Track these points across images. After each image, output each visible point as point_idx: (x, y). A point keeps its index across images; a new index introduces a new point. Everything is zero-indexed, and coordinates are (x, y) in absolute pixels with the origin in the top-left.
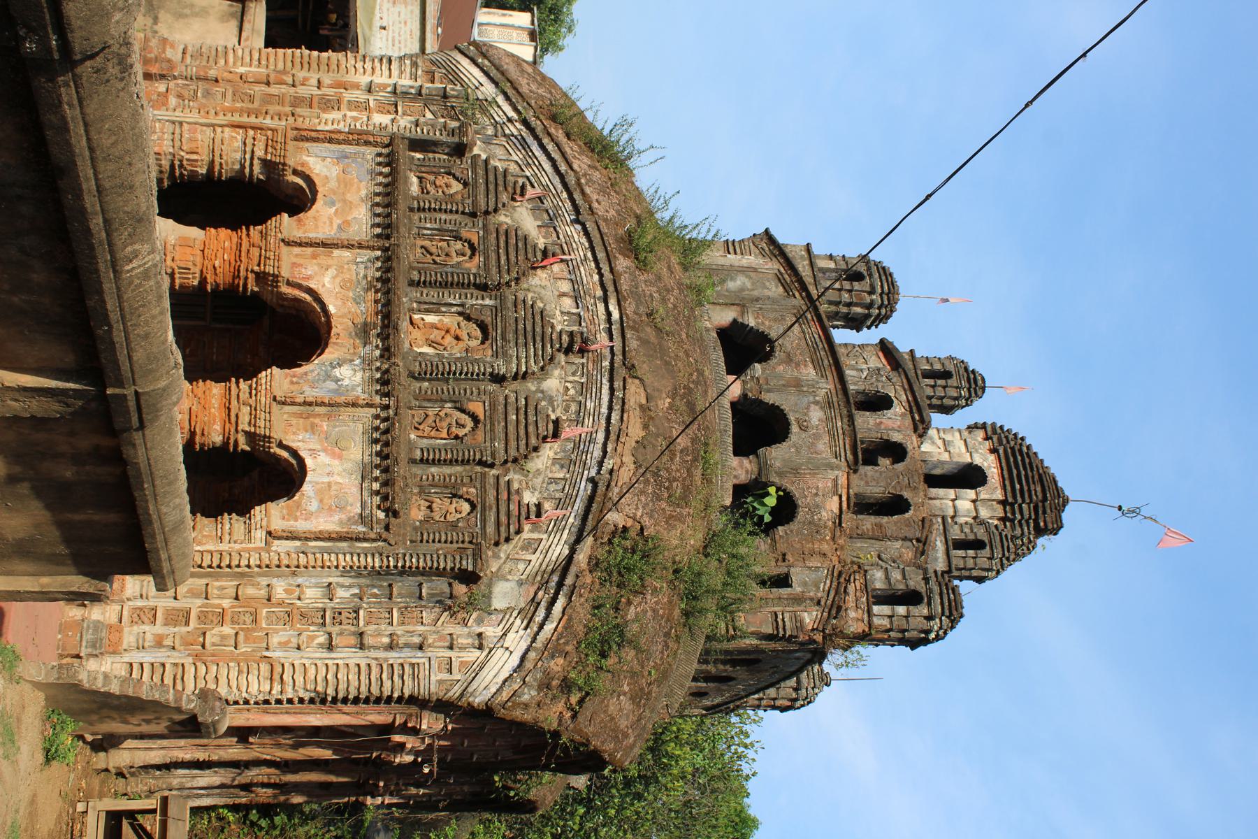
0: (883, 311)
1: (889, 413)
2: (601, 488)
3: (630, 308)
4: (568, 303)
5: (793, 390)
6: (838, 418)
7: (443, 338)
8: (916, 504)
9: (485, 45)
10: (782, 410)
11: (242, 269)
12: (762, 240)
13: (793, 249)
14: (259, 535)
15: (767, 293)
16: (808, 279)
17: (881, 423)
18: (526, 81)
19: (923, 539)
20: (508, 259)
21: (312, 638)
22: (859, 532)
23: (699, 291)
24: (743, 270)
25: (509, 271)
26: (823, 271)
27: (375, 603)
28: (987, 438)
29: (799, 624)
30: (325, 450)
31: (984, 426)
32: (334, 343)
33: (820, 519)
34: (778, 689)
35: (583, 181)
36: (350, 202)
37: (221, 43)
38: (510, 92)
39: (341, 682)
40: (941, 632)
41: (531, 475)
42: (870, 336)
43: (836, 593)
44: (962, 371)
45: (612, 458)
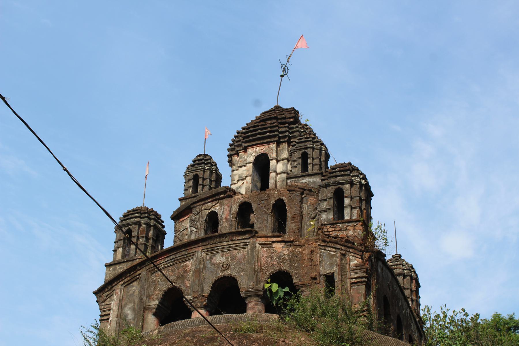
0: (152, 217)
1: (220, 213)
5: (202, 275)
6: (221, 244)
8: (279, 195)
10: (216, 281)
12: (101, 296)
13: (108, 275)
15: (136, 293)
16: (129, 265)
17: (226, 218)
19: (301, 190)
22: (297, 231)
23: (133, 338)
26: (124, 255)
28: (237, 154)
29: (359, 268)
31: (230, 156)
33: (288, 255)
34: (404, 288)
40: (361, 176)
42: (169, 226)
43: (337, 243)
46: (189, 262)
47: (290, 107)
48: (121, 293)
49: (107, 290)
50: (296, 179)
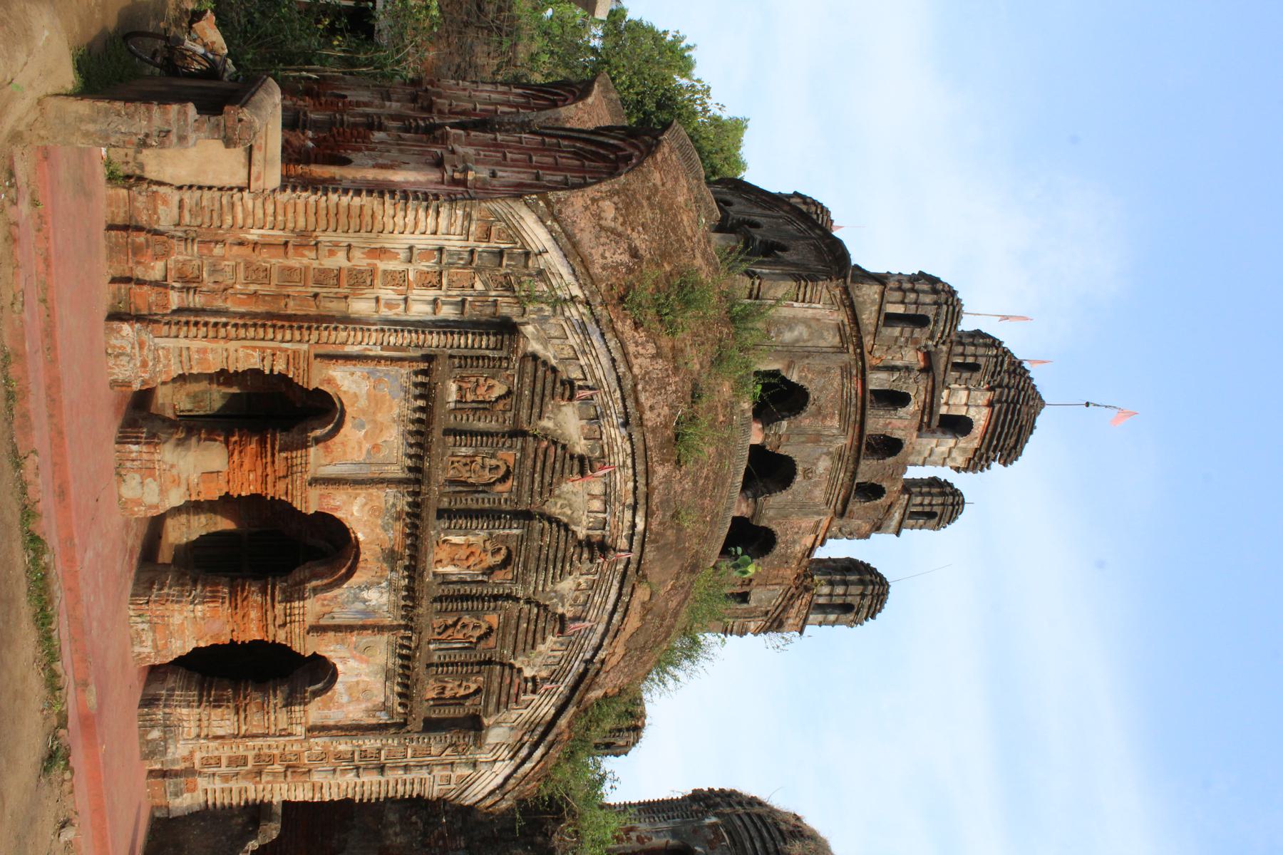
1: (902, 412)
4: (597, 505)
6: (843, 470)
7: (467, 558)
12: (837, 286)
14: (300, 730)
15: (822, 343)
17: (890, 423)
18: (601, 248)
20: (542, 481)
21: (344, 771)
24: (806, 322)
30: (354, 657)
35: (640, 387)
36: (382, 423)
37: (227, 181)
44: (991, 368)
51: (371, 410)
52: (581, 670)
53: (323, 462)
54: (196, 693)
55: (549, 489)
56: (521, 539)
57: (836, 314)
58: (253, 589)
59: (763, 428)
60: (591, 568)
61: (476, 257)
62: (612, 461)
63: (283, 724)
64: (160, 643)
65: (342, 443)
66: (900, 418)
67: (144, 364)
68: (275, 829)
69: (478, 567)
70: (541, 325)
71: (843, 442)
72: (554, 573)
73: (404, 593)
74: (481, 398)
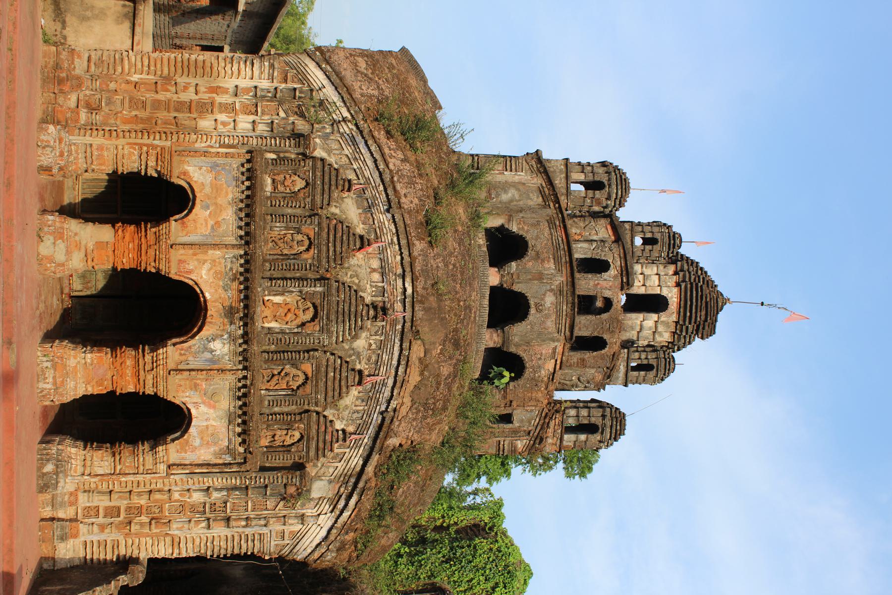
1: (605, 275)
2: (387, 421)
3: (420, 286)
4: (376, 277)
5: (536, 282)
7: (286, 314)
8: (611, 343)
9: (328, 51)
10: (526, 297)
11: (142, 264)
12: (533, 159)
14: (162, 468)
15: (530, 203)
17: (598, 284)
18: (359, 84)
20: (335, 251)
24: (514, 185)
25: (335, 260)
27: (237, 498)
29: (513, 449)
30: (204, 403)
32: (210, 322)
35: (395, 179)
36: (221, 205)
37: (118, 46)
38: (346, 96)
39: (215, 547)
41: (341, 410)
43: (541, 429)
44: (666, 239)
45: (396, 399)
46: (552, 264)
47: (716, 330)
48: (532, 184)
49: (539, 166)
50: (625, 359)
51: (213, 196)
52: (379, 422)
53: (180, 234)
54: (82, 443)
55: (340, 259)
56: (324, 295)
57: (535, 179)
58: (128, 349)
59: (499, 270)
60: (377, 331)
61: (279, 91)
62: (383, 240)
63: (149, 465)
64: (59, 380)
65: (194, 220)
66: (605, 280)
67: (62, 155)
68: (141, 571)
69: (295, 323)
70: (325, 141)
71: (561, 279)
72: (349, 326)
73: (241, 341)
74: (288, 191)
